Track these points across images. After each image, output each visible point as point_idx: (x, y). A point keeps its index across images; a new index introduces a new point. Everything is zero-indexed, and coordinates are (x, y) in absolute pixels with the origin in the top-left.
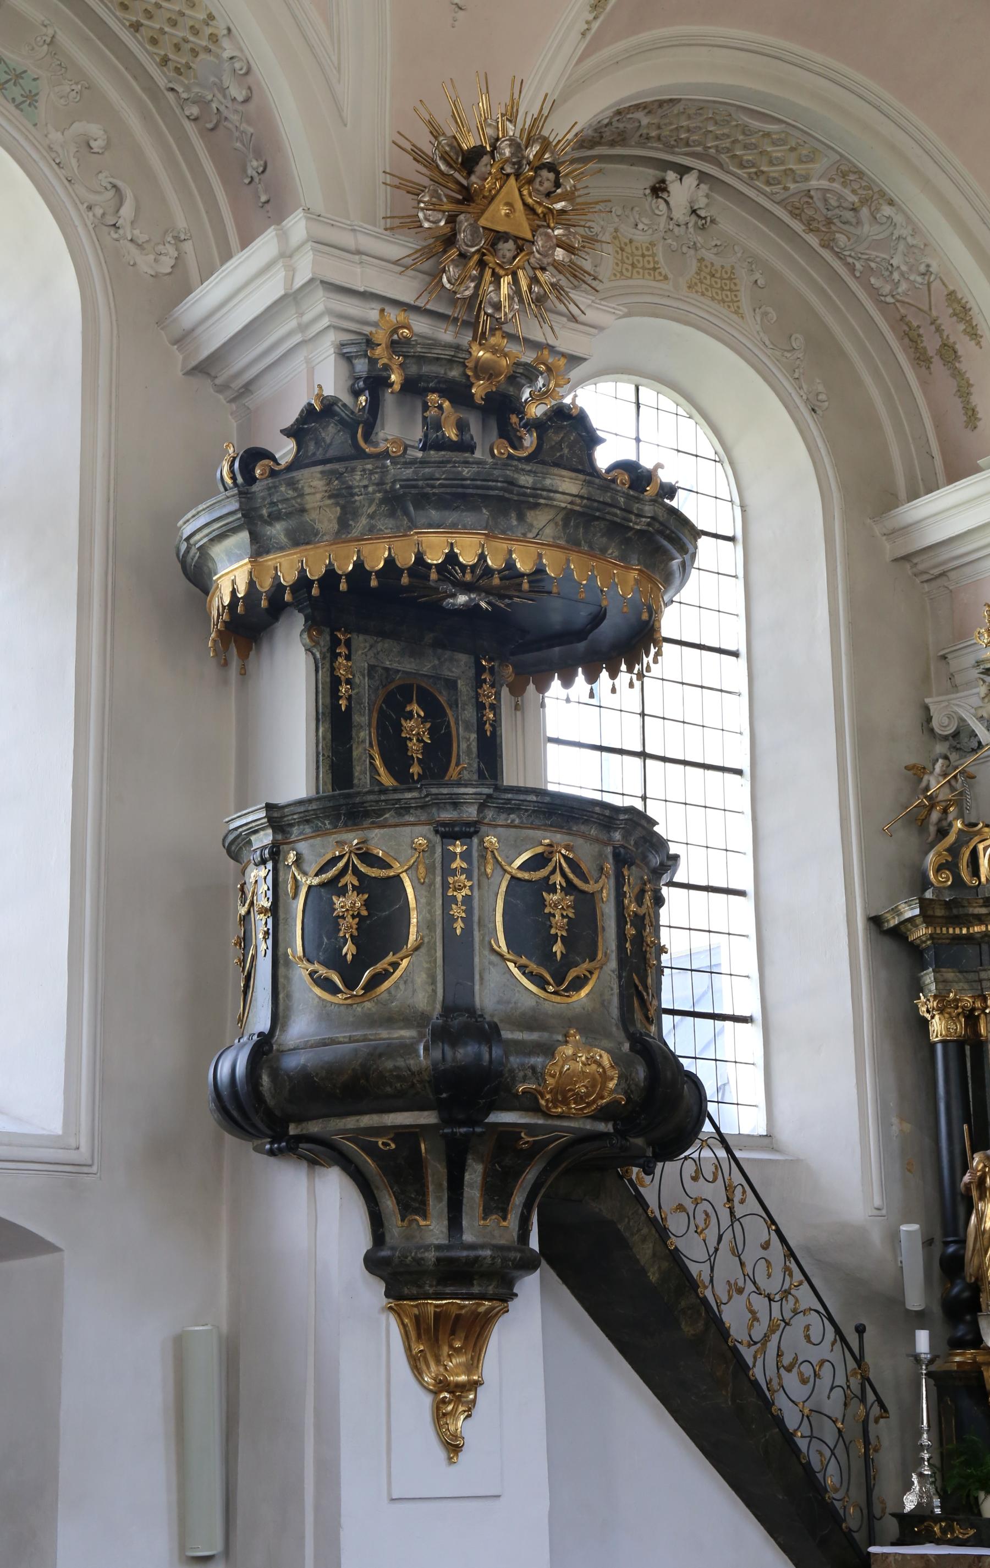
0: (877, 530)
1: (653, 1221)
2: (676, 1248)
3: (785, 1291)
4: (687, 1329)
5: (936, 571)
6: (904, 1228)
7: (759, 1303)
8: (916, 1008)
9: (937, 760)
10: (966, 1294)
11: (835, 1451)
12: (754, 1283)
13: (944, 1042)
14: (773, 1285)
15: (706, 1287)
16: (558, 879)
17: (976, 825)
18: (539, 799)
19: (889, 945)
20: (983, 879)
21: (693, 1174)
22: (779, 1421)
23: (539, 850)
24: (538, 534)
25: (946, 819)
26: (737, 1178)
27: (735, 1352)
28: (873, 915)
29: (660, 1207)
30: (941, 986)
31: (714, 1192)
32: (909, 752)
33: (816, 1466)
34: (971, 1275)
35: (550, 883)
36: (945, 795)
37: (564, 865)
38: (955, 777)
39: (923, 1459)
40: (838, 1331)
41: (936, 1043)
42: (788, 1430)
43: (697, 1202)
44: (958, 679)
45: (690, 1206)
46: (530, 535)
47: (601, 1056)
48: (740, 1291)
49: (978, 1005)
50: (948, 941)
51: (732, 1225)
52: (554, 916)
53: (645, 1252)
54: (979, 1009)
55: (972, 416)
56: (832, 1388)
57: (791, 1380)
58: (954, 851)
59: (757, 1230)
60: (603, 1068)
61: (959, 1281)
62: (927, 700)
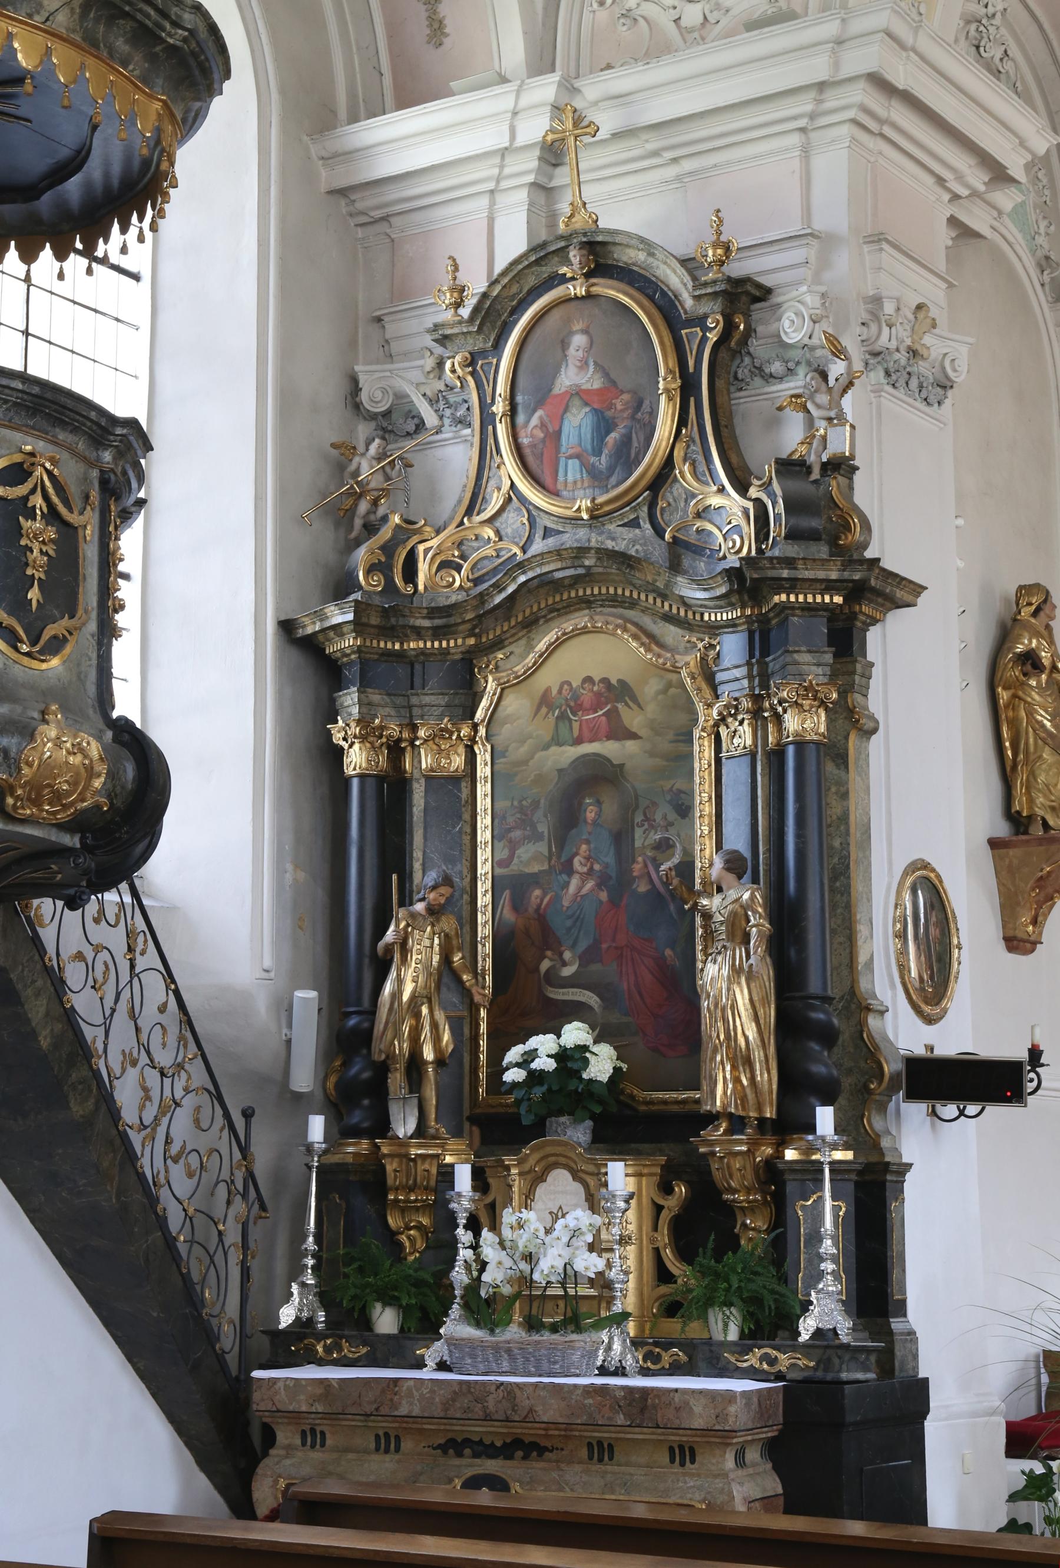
0: (314, 150)
1: (48, 970)
2: (72, 1006)
3: (179, 1065)
4: (78, 1109)
5: (377, 214)
6: (299, 994)
7: (153, 1077)
8: (329, 735)
9: (374, 440)
10: (366, 1075)
11: (216, 1258)
12: (148, 1053)
13: (362, 777)
14: (165, 1058)
15: (100, 1057)
16: (38, 501)
17: (415, 523)
18: (25, 388)
19: (295, 655)
20: (421, 587)
21: (96, 915)
22: (162, 1222)
23: (18, 458)
24: (47, 20)
25: (375, 513)
26: (141, 925)
27: (124, 1138)
28: (282, 618)
29: (58, 954)
30: (364, 710)
31: (116, 939)
32: (329, 426)
33: (196, 1277)
34: (381, 1051)
35: (30, 505)
37: (47, 483)
38: (394, 460)
39: (306, 1266)
40: (227, 1115)
42: (170, 1233)
43: (98, 949)
44: (395, 348)
45: (89, 955)
46: (37, 18)
47: (88, 743)
48: (134, 1063)
49: (406, 735)
50: (376, 657)
51: (131, 982)
52: (32, 552)
53: (37, 1009)
54: (406, 740)
55: (437, 30)
56: (217, 1183)
57: (177, 1171)
58: (388, 549)
59: (155, 988)
60: (91, 761)
61: (357, 1059)
62: (357, 368)
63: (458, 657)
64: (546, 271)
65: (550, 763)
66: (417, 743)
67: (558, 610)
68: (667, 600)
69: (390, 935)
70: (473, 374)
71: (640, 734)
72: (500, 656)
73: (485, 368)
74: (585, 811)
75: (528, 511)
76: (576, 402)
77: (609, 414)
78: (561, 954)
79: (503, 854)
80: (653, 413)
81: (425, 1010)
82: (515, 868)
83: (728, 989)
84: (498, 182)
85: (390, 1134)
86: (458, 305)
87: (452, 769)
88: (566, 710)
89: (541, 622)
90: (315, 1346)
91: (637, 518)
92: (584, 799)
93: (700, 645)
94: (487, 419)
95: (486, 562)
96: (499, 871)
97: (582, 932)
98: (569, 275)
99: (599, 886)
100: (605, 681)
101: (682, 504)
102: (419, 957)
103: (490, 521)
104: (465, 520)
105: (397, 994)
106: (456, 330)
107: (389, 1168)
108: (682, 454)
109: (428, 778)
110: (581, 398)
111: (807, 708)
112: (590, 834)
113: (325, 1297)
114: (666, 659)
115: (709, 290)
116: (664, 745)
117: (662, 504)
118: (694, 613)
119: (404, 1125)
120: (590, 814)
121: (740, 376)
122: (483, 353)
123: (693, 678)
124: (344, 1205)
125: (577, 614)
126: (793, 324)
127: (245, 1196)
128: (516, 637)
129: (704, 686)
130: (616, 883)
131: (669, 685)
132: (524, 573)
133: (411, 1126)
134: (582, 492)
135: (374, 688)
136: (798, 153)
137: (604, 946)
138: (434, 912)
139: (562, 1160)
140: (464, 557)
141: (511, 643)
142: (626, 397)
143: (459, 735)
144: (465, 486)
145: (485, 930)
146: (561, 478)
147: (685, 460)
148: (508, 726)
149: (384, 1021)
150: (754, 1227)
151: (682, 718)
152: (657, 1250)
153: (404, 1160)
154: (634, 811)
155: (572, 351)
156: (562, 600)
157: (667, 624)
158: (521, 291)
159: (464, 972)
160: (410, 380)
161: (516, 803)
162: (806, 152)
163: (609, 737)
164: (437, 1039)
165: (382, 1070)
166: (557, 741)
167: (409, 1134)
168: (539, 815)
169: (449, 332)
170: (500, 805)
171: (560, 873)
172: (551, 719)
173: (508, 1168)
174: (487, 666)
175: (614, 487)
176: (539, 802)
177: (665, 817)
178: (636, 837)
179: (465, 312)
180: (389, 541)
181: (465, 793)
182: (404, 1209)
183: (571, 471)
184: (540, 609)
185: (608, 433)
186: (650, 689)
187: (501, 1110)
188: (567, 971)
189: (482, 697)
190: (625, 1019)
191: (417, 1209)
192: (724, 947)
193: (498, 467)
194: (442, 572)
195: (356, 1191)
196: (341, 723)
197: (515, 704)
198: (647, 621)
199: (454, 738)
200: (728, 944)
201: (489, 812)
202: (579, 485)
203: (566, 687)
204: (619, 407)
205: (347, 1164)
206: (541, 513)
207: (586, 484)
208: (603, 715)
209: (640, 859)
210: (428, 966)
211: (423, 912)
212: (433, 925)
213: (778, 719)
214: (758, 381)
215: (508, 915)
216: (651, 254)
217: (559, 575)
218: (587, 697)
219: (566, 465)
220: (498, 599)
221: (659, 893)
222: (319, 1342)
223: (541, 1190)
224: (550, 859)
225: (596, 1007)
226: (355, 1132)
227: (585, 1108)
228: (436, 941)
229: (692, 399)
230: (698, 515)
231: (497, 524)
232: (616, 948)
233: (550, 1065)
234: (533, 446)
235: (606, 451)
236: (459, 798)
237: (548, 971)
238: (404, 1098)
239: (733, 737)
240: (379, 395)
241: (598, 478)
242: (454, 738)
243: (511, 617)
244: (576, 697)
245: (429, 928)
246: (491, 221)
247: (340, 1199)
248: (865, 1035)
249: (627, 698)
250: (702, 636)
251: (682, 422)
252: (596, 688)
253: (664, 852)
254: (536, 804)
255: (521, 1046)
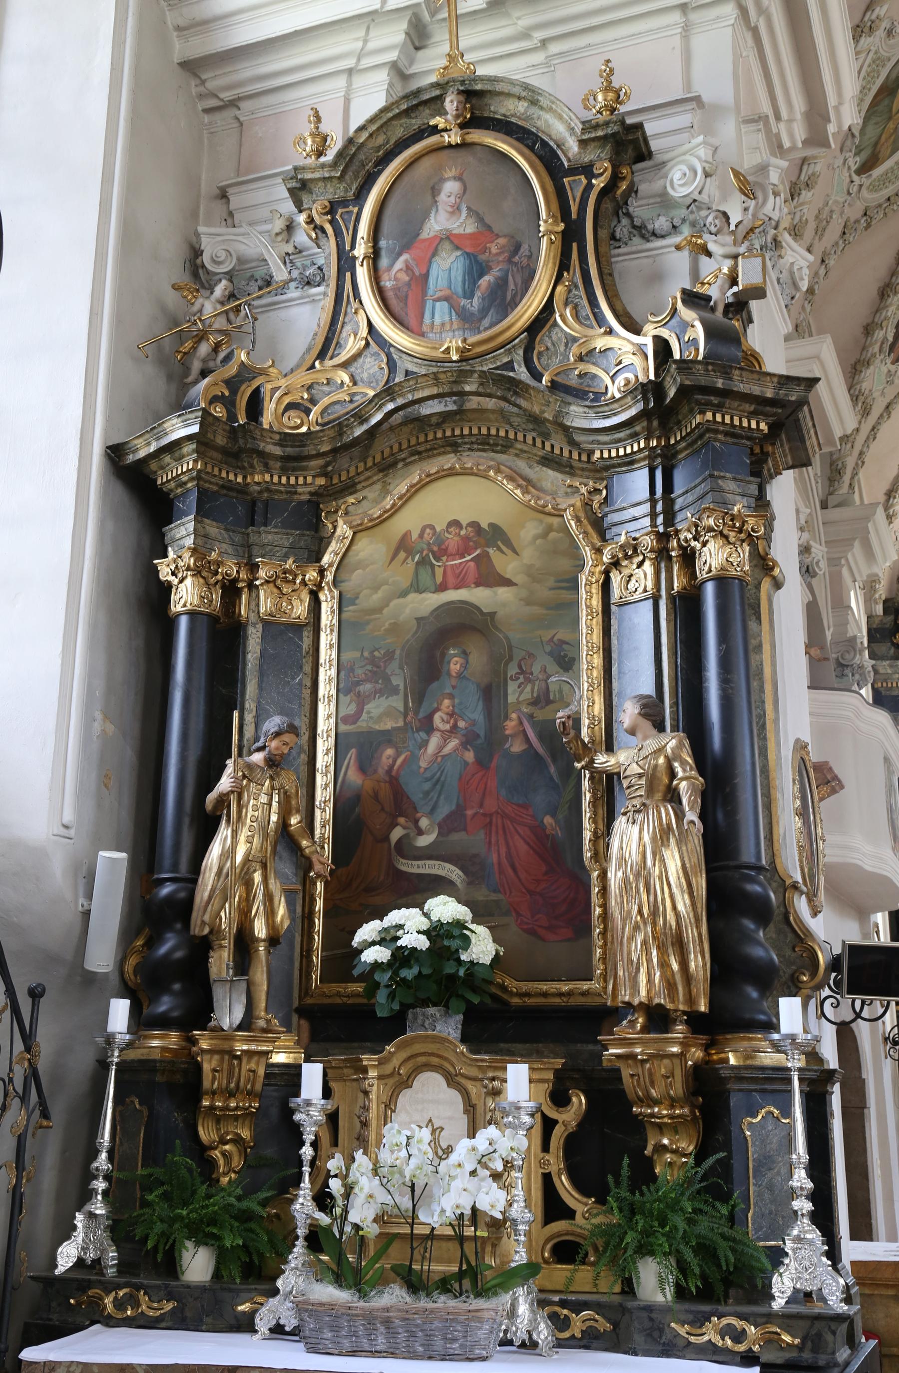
5: (226, 95)
6: (103, 854)
10: (179, 954)
19: (120, 491)
34: (203, 923)
36: (220, 323)
38: (240, 305)
39: (95, 1191)
41: (179, 614)
49: (243, 575)
50: (215, 488)
54: (243, 581)
61: (169, 935)
62: (201, 229)
63: (306, 497)
64: (415, 123)
65: (407, 611)
66: (258, 583)
67: (419, 453)
68: (547, 439)
69: (225, 783)
70: (332, 222)
71: (514, 580)
72: (351, 500)
73: (346, 217)
74: (449, 663)
75: (389, 356)
76: (447, 245)
77: (482, 257)
78: (416, 822)
79: (349, 709)
80: (533, 257)
81: (257, 877)
82: (364, 724)
83: (654, 854)
84: (359, 60)
85: (212, 1024)
86: (320, 154)
87: (293, 616)
88: (427, 555)
89: (400, 465)
90: (102, 1299)
91: (511, 362)
92: (448, 649)
93: (584, 490)
94: (346, 263)
95: (337, 407)
96: (343, 728)
97: (442, 797)
98: (441, 126)
99: (465, 745)
100: (475, 525)
101: (562, 348)
102: (256, 814)
103: (345, 365)
104: (317, 363)
105: (229, 854)
106: (317, 175)
107: (206, 1067)
108: (564, 296)
109: (266, 624)
110: (452, 242)
111: (732, 540)
112: (454, 687)
113: (119, 1229)
114: (546, 501)
115: (600, 133)
116: (544, 592)
117: (539, 348)
118: (580, 455)
119: (229, 1012)
120: (455, 666)
121: (618, 236)
122: (344, 203)
123: (578, 520)
124: (146, 1113)
125: (440, 458)
126: (681, 180)
127: (24, 1098)
128: (371, 481)
129: (590, 529)
130: (486, 743)
131: (550, 529)
132: (393, 400)
133: (238, 1014)
134: (451, 334)
135: (213, 520)
136: (679, 30)
137: (469, 813)
138: (272, 763)
139: (435, 1060)
140: (313, 401)
141: (364, 488)
142: (502, 241)
143: (303, 580)
144: (316, 334)
145: (323, 793)
146: (427, 320)
147: (566, 304)
148: (359, 571)
149: (209, 888)
150: (673, 1152)
151: (565, 564)
152: (547, 1179)
153: (226, 1057)
154: (506, 664)
155: (442, 197)
156: (427, 441)
157: (544, 469)
158: (387, 143)
159: (303, 838)
160: (257, 243)
161: (366, 654)
162: (687, 30)
163: (478, 584)
164: (270, 913)
165: (202, 947)
166: (417, 587)
167: (235, 1026)
168: (394, 665)
169: (308, 176)
170: (347, 656)
171: (418, 731)
172: (411, 565)
173: (365, 1070)
174: (336, 512)
175: (486, 329)
176: (394, 652)
177: (544, 670)
178: (510, 691)
179: (330, 156)
180: (233, 377)
181: (307, 642)
182: (219, 1118)
183: (440, 313)
184: (401, 450)
185: (481, 276)
186: (527, 533)
187: (338, 1001)
188: (423, 841)
189: (329, 543)
190: (494, 897)
191: (236, 1118)
192: (644, 805)
193: (356, 313)
194: (292, 413)
195: (164, 1095)
196: (171, 554)
197: (369, 549)
198: (521, 465)
199: (298, 581)
200: (647, 802)
201: (335, 663)
202: (447, 327)
203: (428, 531)
204: (494, 250)
205: (154, 1061)
206: (404, 356)
207: (455, 326)
208: (472, 560)
209: (514, 716)
210: (264, 828)
211: (262, 764)
212: (272, 779)
213: (689, 558)
214: (637, 240)
215: (353, 777)
216: (534, 103)
217: (427, 409)
218: (452, 540)
219: (434, 308)
220: (358, 432)
221: (536, 753)
222: (108, 1293)
223: (405, 1098)
224: (405, 715)
225: (458, 882)
226: (163, 1023)
227: (458, 996)
228: (276, 798)
229: (575, 245)
230: (581, 359)
231: (352, 369)
232: (484, 815)
233: (423, 943)
234: (396, 289)
235: (478, 294)
236: (300, 647)
237: (400, 841)
238: (232, 981)
239: (628, 582)
240: (223, 256)
241: (468, 320)
242: (298, 581)
243: (367, 457)
244: (440, 540)
245: (267, 783)
246: (347, 101)
247: (140, 1104)
248: (791, 918)
249: (499, 543)
250: (585, 480)
251: (563, 266)
252: (463, 532)
253: (542, 708)
254: (389, 656)
255: (377, 922)
